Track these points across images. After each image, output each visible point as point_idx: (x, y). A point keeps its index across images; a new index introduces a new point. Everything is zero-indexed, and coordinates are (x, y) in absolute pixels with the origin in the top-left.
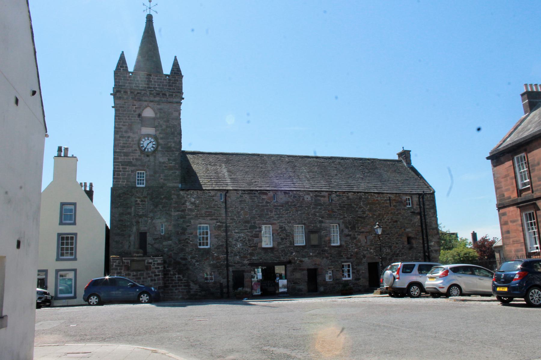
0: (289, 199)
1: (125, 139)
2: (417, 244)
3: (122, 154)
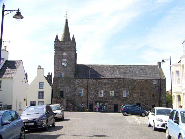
2: (157, 97)
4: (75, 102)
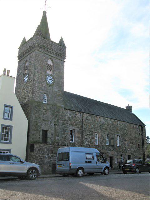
1: (39, 74)
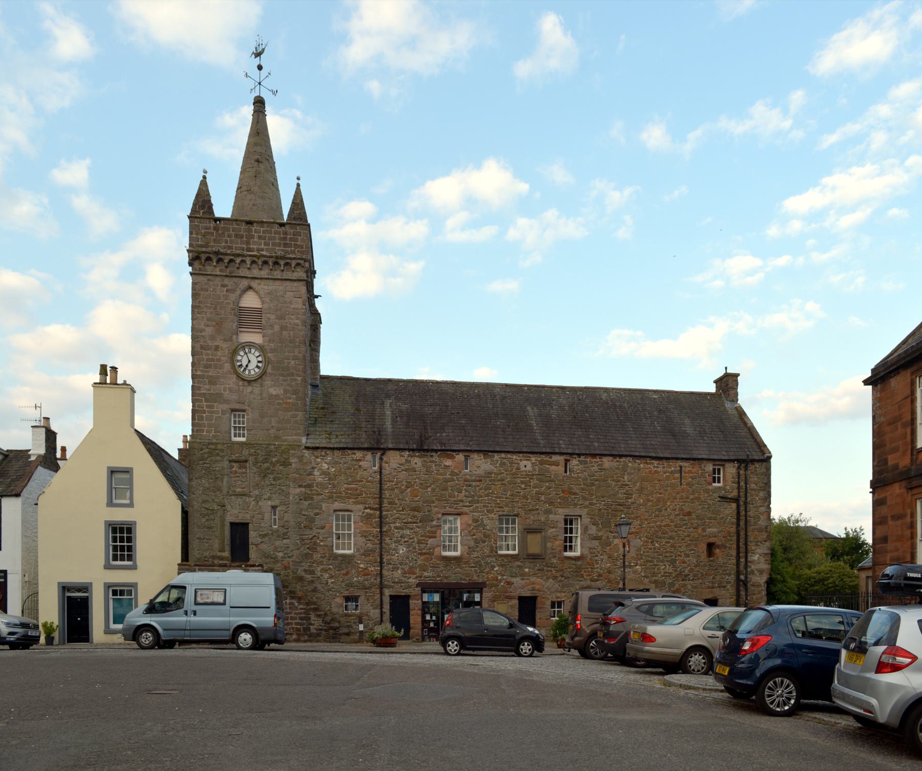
0: (492, 467)
2: (726, 558)
3: (207, 380)
4: (315, 590)
